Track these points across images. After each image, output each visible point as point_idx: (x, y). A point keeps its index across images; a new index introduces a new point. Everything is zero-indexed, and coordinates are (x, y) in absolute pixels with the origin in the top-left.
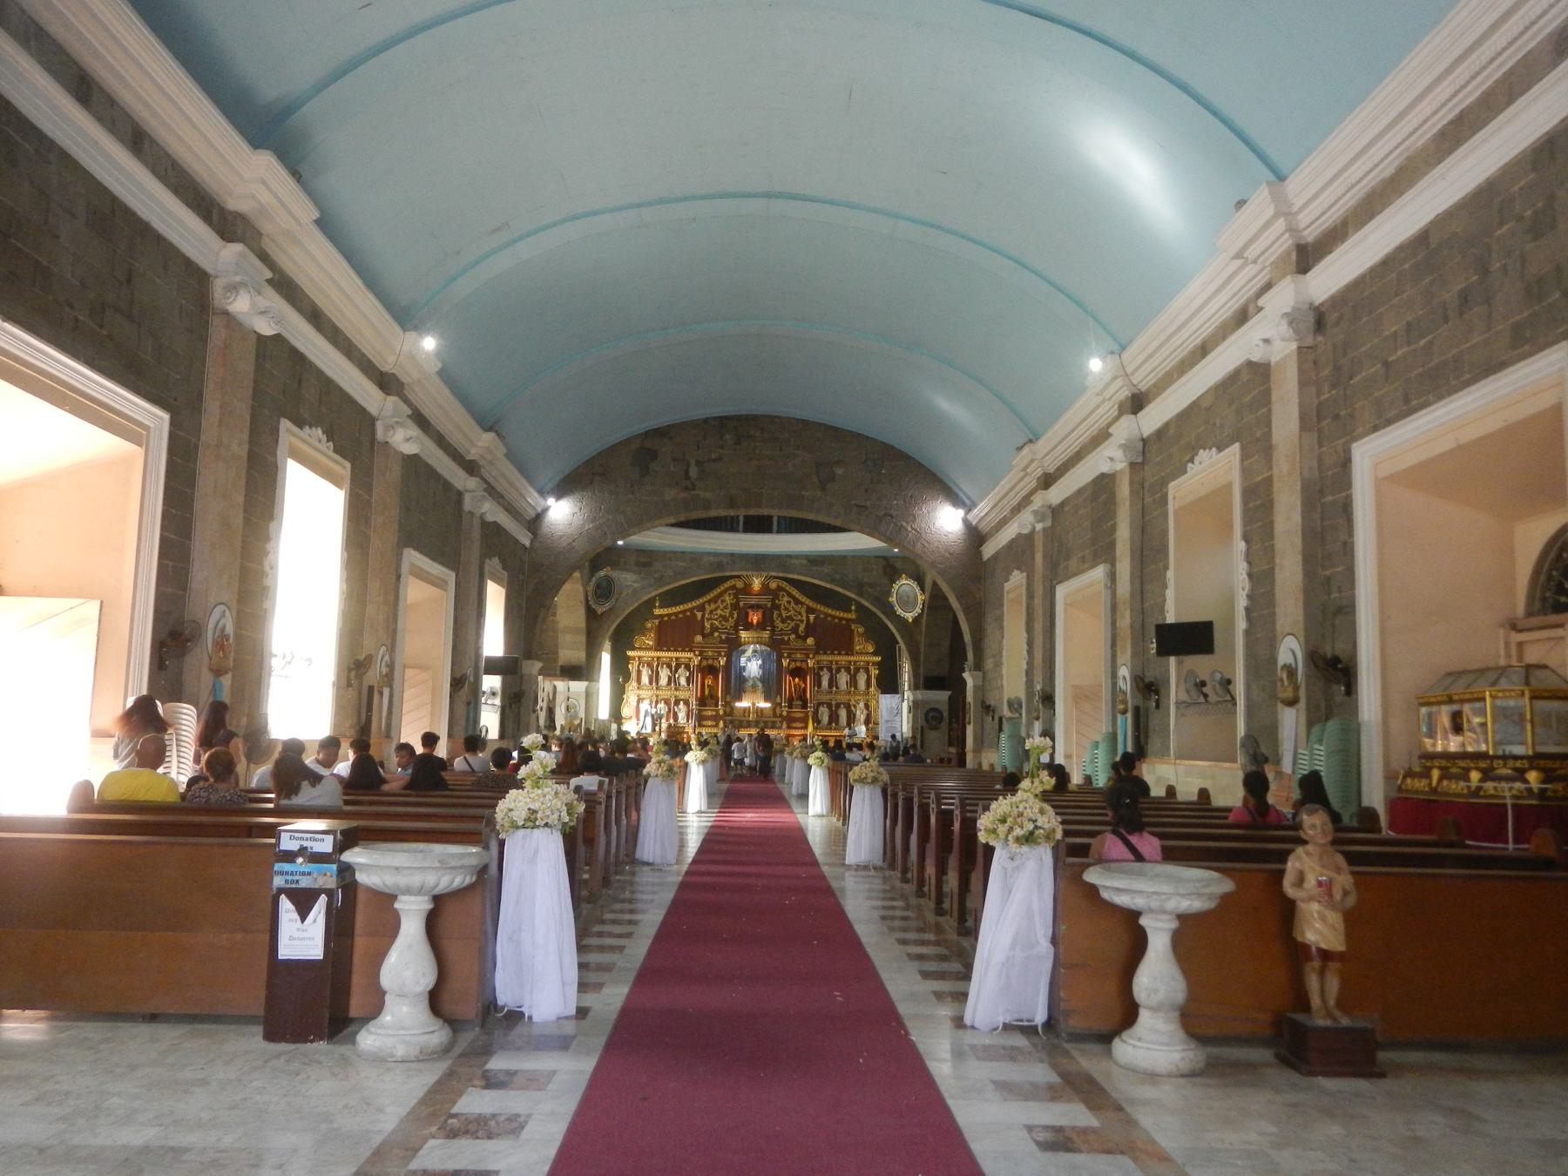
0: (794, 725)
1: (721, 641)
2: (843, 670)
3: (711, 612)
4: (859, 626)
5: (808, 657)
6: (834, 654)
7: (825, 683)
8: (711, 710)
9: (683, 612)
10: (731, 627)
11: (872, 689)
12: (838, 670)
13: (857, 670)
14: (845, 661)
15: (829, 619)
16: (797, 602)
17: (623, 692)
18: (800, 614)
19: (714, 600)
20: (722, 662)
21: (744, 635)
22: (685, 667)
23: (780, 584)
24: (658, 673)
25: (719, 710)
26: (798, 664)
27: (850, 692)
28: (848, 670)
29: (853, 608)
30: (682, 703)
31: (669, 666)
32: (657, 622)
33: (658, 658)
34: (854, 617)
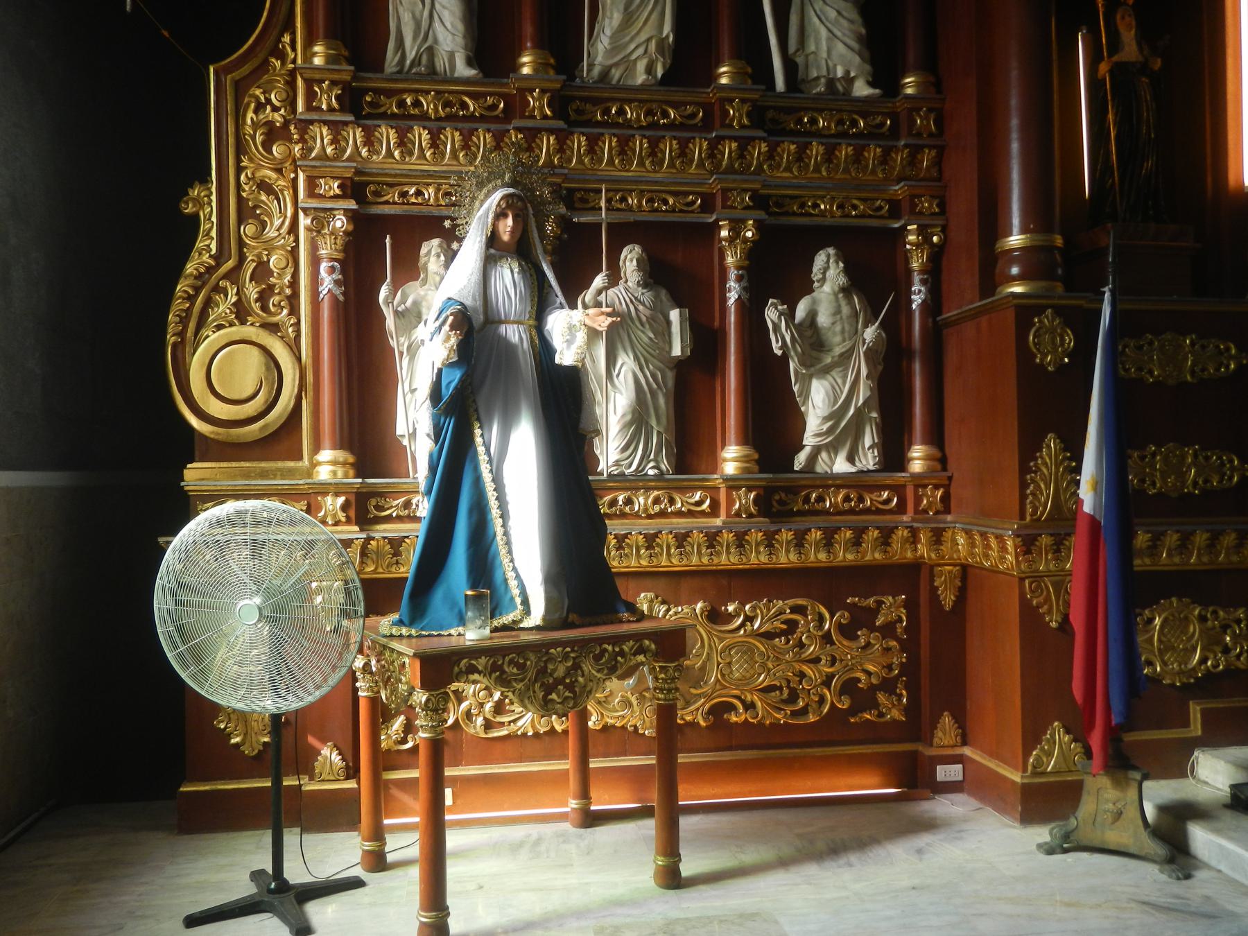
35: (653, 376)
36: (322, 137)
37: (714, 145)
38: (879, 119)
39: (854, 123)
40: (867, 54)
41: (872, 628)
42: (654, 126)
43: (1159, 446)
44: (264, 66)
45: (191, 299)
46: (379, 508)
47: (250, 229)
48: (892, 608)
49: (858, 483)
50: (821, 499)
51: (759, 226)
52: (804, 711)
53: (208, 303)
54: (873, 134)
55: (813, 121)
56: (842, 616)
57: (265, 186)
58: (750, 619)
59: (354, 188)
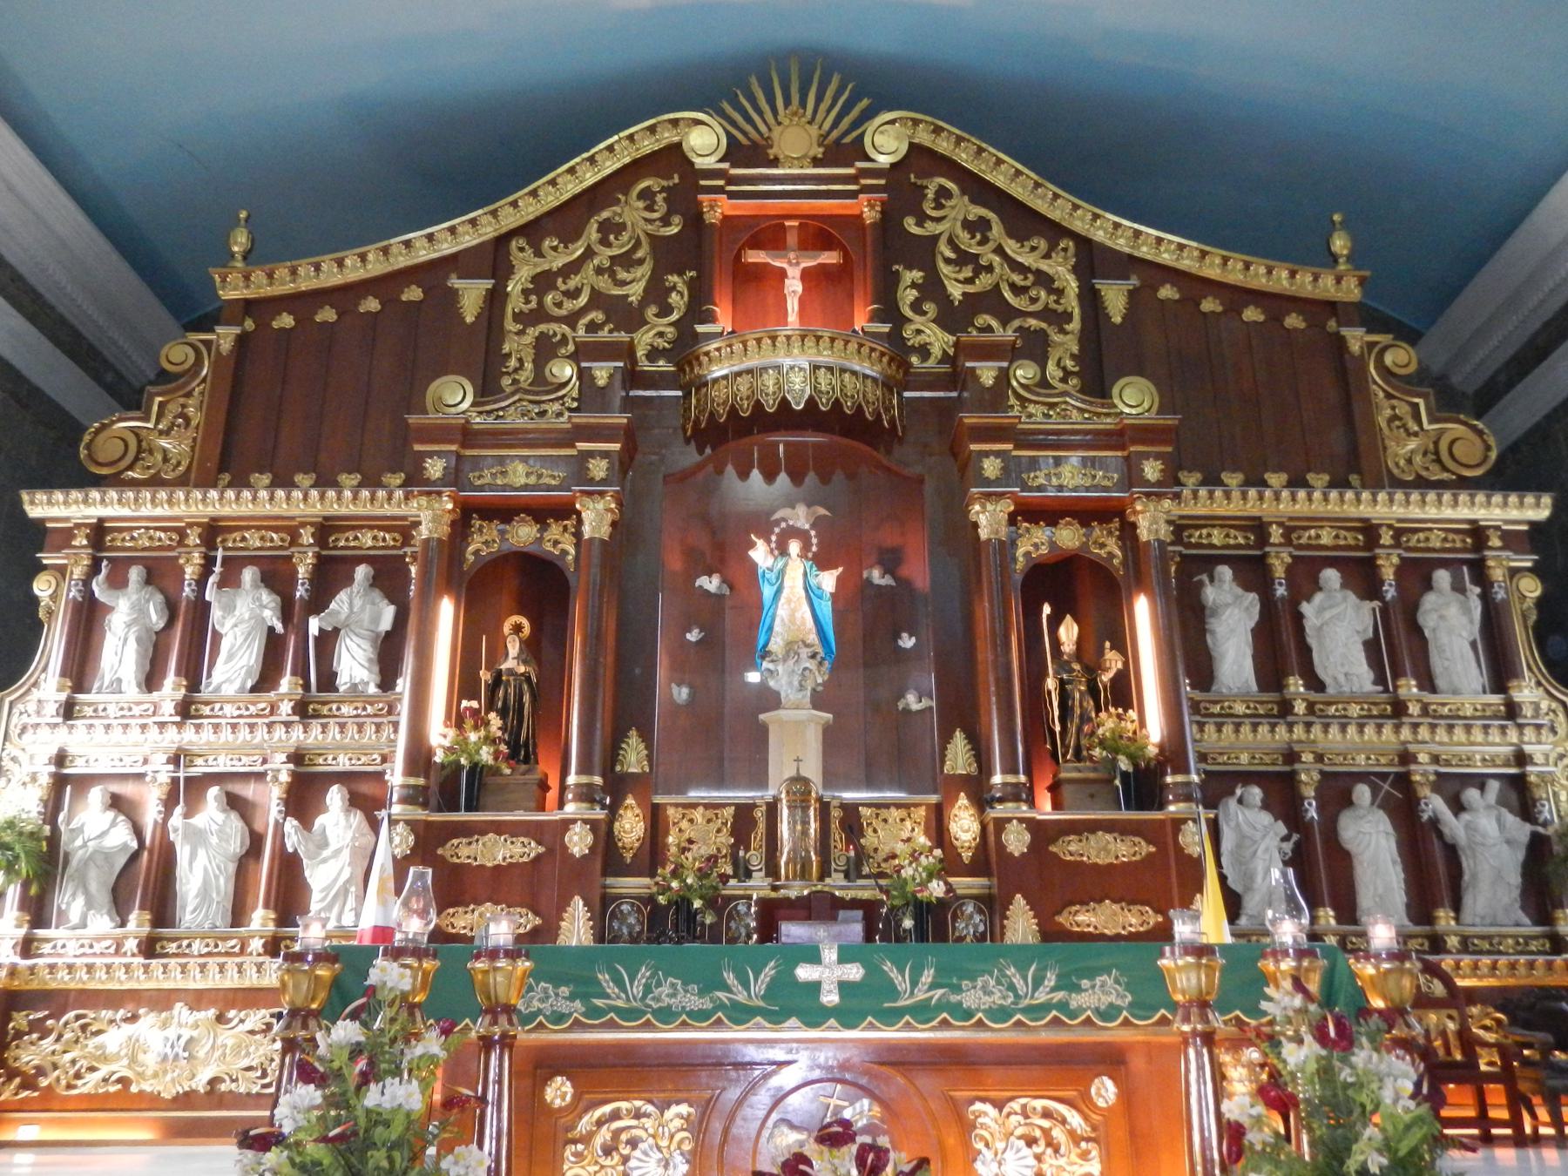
0: (1085, 919)
1: (591, 397)
2: (1331, 576)
3: (543, 282)
6: (1265, 484)
8: (514, 830)
9: (386, 285)
11: (1527, 692)
12: (1305, 576)
13: (1417, 574)
15: (1209, 305)
16: (1024, 221)
18: (1044, 280)
22: (376, 582)
23: (924, 137)
24: (201, 609)
25: (566, 824)
26: (1068, 536)
27: (1399, 709)
28: (1363, 578)
29: (1340, 244)
30: (335, 796)
31: (276, 576)
32: (225, 335)
33: (213, 531)
34: (1351, 291)
35: (219, 868)
36: (44, 732)
37: (270, 726)
38: (381, 705)
39: (364, 709)
40: (376, 669)
42: (240, 716)
43: (479, 903)
46: (38, 948)
51: (294, 774)
54: (376, 715)
55: (339, 709)
57: (14, 759)
58: (242, 1021)
59: (61, 759)
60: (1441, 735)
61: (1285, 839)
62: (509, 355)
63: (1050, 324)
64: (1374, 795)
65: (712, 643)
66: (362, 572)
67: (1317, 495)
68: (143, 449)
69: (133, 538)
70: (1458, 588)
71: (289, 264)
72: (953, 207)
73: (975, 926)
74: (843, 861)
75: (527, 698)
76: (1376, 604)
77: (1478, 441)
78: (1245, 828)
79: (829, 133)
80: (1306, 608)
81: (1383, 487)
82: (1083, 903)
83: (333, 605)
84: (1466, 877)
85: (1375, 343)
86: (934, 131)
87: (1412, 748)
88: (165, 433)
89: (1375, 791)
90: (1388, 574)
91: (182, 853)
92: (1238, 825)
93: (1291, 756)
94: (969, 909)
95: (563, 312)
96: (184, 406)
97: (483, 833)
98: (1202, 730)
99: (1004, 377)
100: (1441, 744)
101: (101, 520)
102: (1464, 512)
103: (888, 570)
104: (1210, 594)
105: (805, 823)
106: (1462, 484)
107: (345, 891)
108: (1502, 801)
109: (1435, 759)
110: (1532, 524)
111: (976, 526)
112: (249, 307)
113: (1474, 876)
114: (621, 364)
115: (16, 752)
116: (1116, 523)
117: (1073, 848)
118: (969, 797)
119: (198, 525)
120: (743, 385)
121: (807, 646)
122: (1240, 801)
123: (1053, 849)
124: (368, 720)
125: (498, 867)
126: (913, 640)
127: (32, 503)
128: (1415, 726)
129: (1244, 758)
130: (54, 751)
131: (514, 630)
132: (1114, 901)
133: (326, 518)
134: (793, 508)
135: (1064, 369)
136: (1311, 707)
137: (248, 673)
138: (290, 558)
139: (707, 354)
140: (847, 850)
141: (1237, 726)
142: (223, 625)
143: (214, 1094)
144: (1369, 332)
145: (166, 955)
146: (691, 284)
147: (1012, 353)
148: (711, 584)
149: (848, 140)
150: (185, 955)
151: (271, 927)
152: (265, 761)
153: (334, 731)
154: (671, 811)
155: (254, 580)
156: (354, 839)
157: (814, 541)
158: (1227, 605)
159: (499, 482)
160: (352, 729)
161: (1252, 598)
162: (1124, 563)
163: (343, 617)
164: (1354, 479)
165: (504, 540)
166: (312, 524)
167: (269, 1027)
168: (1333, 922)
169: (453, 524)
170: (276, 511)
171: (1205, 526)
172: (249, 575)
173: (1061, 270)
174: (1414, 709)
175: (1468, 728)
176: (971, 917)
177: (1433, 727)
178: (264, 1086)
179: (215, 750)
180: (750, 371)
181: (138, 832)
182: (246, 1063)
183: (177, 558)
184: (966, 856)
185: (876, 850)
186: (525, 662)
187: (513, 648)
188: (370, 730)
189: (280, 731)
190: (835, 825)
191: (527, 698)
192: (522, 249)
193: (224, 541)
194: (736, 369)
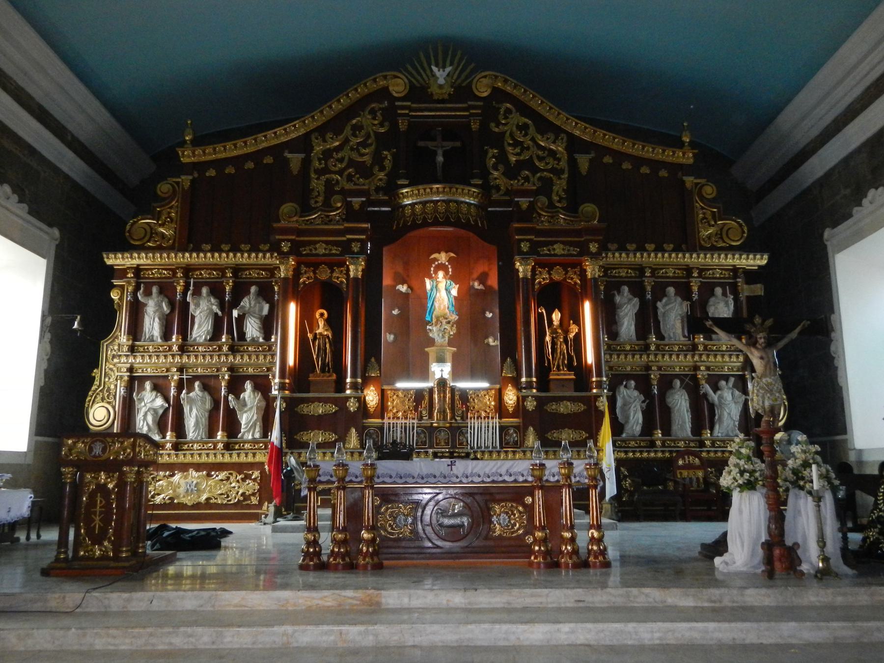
1: (351, 214)
2: (671, 290)
3: (327, 154)
4: (703, 181)
5: (584, 251)
6: (645, 250)
7: (627, 326)
8: (325, 401)
10: (378, 189)
12: (659, 292)
14: (677, 267)
16: (545, 126)
17: (95, 364)
18: (553, 153)
19: (334, 125)
20: (356, 270)
21: (409, 198)
24: (185, 306)
25: (347, 398)
26: (558, 275)
27: (694, 348)
28: (684, 291)
30: (248, 386)
31: (216, 291)
32: (185, 180)
33: (188, 270)
36: (124, 359)
37: (219, 356)
40: (262, 331)
41: (251, 479)
43: (313, 430)
44: (114, 340)
45: (92, 396)
47: (107, 380)
48: (256, 474)
49: (254, 442)
50: (243, 446)
51: (230, 376)
52: (230, 500)
53: (95, 397)
54: (263, 351)
55: (247, 348)
56: (242, 476)
57: (111, 369)
58: (217, 476)
59: (131, 370)
60: (711, 358)
61: (644, 402)
62: (313, 190)
63: (554, 175)
64: (681, 384)
65: (404, 317)
66: (253, 289)
67: (666, 255)
68: (151, 233)
69: (152, 273)
70: (724, 294)
71: (212, 146)
72: (512, 118)
73: (514, 438)
74: (460, 412)
75: (328, 346)
76: (689, 303)
77: (740, 230)
78: (626, 397)
79: (456, 80)
80: (659, 304)
81: (696, 251)
82: (557, 429)
83: (242, 304)
84: (716, 417)
85: (699, 183)
86: (504, 81)
87: (698, 364)
88: (162, 225)
89: (682, 381)
90: (695, 289)
91: (186, 409)
92: (624, 396)
93: (648, 368)
94: (512, 431)
95: (337, 169)
96: (169, 213)
97: (313, 402)
98: (611, 357)
99: (532, 205)
100: (711, 362)
101: (138, 265)
102: (730, 261)
103: (481, 283)
104: (618, 299)
105: (445, 397)
106: (731, 249)
107: (255, 425)
108: (735, 386)
109: (708, 368)
110: (759, 266)
111: (518, 271)
112: (195, 166)
113: (720, 418)
114: (364, 199)
115: (111, 366)
116: (577, 270)
117: (554, 407)
118: (513, 386)
119: (182, 268)
120: (418, 208)
121: (446, 319)
122: (626, 386)
123: (545, 408)
124: (261, 353)
125: (320, 416)
126: (491, 314)
127: (108, 258)
128: (701, 355)
129: (629, 368)
130: (128, 366)
131: (320, 316)
132: (570, 428)
133: (237, 265)
134: (440, 253)
135: (560, 196)
136: (658, 347)
137: (208, 333)
138: (223, 282)
139: (402, 193)
140: (462, 407)
141: (626, 355)
142: (195, 312)
143: (208, 504)
144: (696, 178)
145: (183, 450)
146: (394, 156)
147: (536, 193)
148: (403, 288)
149: (464, 85)
150: (191, 450)
151: (226, 439)
152: (217, 371)
153: (246, 358)
154: (389, 392)
155: (207, 292)
156: (258, 403)
157: (450, 270)
158: (625, 304)
159: (314, 252)
160: (254, 357)
161: (636, 300)
162: (581, 286)
163: (247, 309)
164: (684, 246)
165: (316, 277)
166: (231, 268)
167: (228, 479)
168: (660, 435)
169: (294, 270)
170: (215, 261)
171: (618, 268)
172: (205, 290)
173: (559, 148)
174: (701, 348)
175: (723, 356)
176: (512, 434)
177: (708, 356)
178: (228, 501)
179: (196, 366)
180: (420, 203)
181: (166, 399)
182: (219, 492)
183: (173, 282)
184: (511, 410)
185: (474, 408)
186: (327, 330)
187: (321, 323)
188: (261, 358)
189: (223, 358)
190: (457, 397)
191: (328, 346)
192: (317, 139)
193: (192, 275)
194: (414, 201)
